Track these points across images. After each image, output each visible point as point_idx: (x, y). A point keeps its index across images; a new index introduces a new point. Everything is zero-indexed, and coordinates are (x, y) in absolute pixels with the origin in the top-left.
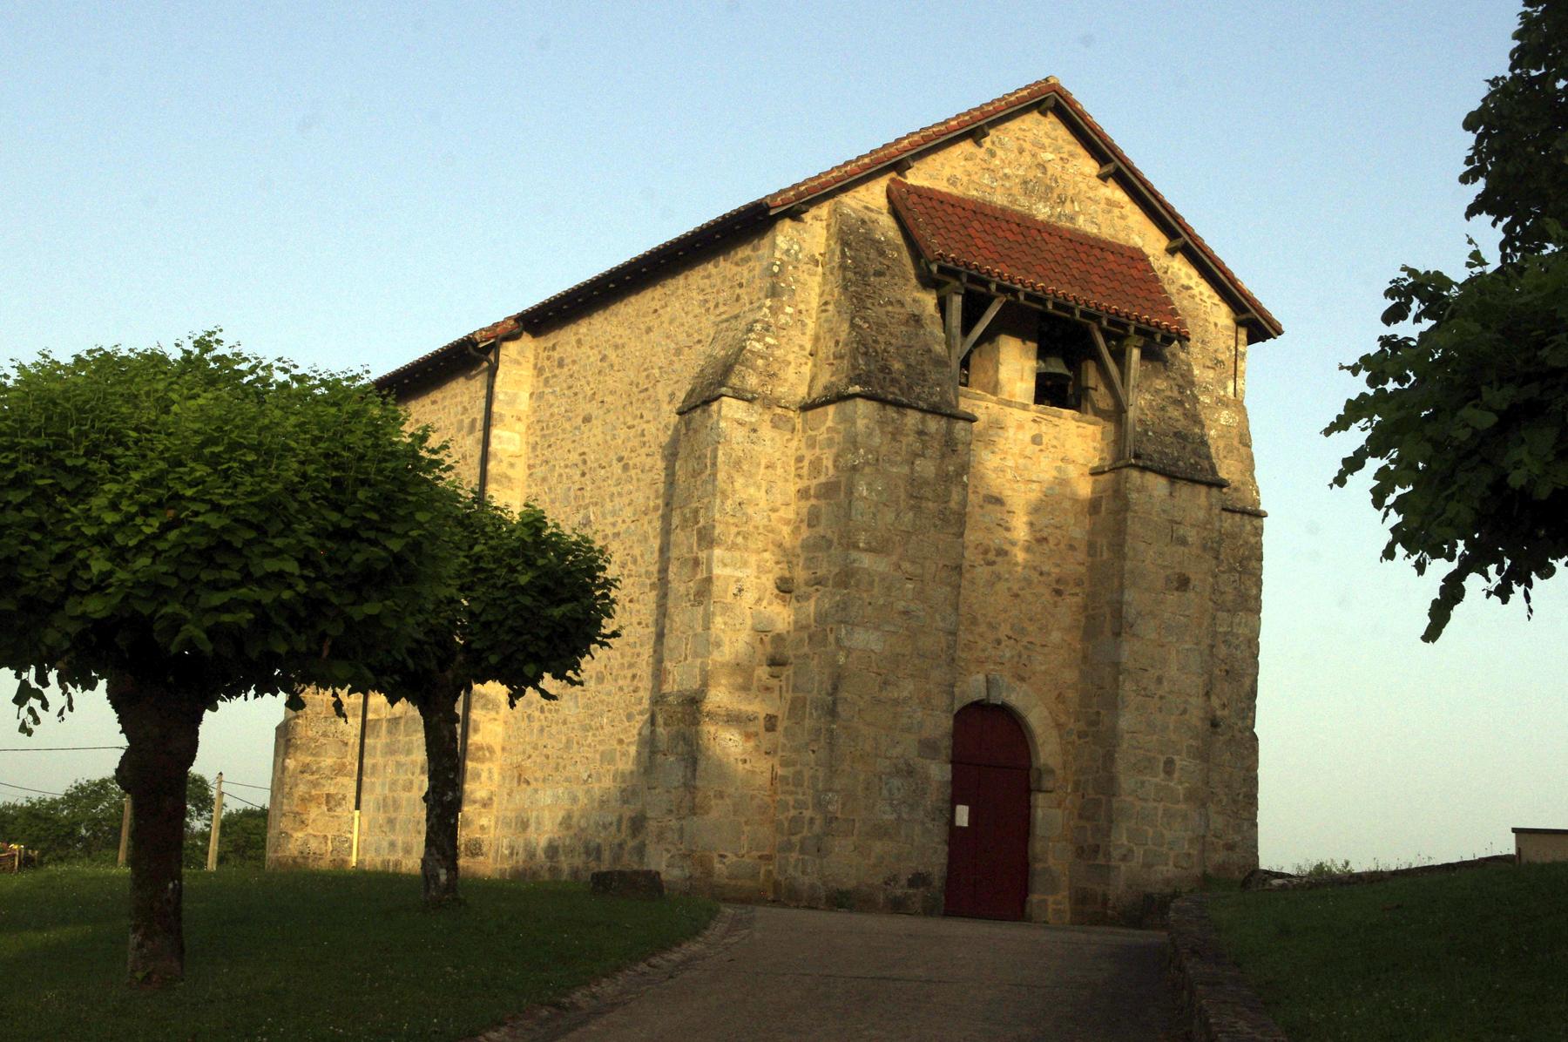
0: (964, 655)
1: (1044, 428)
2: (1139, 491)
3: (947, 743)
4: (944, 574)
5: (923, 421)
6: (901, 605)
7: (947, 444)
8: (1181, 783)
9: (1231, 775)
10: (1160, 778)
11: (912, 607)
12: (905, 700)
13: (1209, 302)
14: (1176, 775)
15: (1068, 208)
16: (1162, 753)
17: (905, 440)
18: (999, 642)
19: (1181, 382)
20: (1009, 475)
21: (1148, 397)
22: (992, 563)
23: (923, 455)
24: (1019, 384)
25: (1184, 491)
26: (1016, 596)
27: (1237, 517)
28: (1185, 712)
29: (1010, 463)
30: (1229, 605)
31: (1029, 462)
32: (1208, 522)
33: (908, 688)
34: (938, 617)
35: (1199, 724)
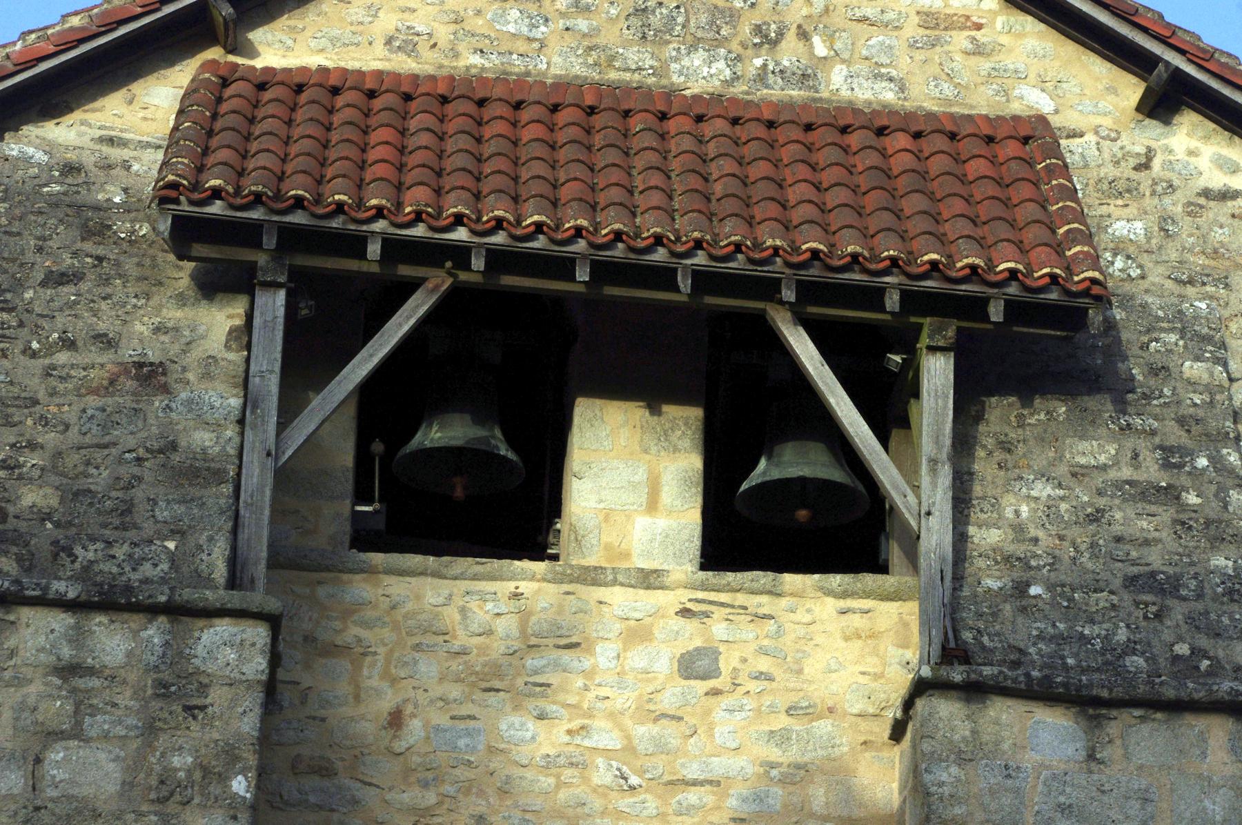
1: (719, 629)
2: (962, 759)
5: (78, 637)
7: (163, 690)
15: (789, 54)
19: (1175, 435)
20: (603, 775)
21: (1043, 490)
23: (76, 733)
25: (1141, 743)
31: (669, 730)
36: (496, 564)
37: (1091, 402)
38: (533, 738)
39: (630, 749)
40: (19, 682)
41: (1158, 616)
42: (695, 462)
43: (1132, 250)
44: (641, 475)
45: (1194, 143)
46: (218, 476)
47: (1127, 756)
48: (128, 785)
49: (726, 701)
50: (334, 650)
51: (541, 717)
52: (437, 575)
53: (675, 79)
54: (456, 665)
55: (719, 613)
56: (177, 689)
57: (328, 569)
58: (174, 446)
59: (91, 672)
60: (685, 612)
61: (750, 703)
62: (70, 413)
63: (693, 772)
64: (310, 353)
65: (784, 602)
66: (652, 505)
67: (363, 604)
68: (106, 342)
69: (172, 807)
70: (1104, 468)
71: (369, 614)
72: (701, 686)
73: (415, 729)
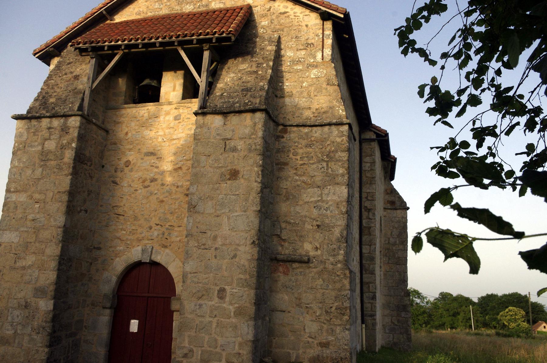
0: (129, 237)
3: (52, 288)
4: (57, 196)
5: (50, 123)
6: (30, 217)
8: (231, 304)
9: (323, 294)
10: (215, 301)
11: (38, 216)
12: (30, 267)
13: (301, 16)
14: (227, 299)
16: (216, 285)
17: (40, 134)
18: (151, 228)
19: (261, 61)
20: (160, 139)
21: (232, 75)
22: (149, 186)
23: (49, 139)
24: (172, 93)
25: (234, 119)
26: (162, 201)
27: (326, 129)
28: (235, 256)
29: (161, 133)
30: (319, 183)
31: (172, 130)
32: (252, 134)
33: (30, 260)
34: (52, 220)
35: (246, 264)
36: (144, 104)
37: (246, 57)
38: (149, 134)
39: (165, 135)
40: (42, 131)
41: (245, 96)
42: (182, 81)
43: (265, 27)
44: (172, 85)
45: (279, 4)
46: (81, 93)
47: (231, 123)
48: (56, 147)
49: (182, 124)
50: (119, 123)
51: (151, 130)
52: (136, 107)
53: (184, 10)
54: (138, 123)
55: (181, 108)
56: (65, 130)
57: (118, 109)
58: (76, 88)
59: (52, 128)
60: (176, 108)
61: (185, 124)
62: (63, 86)
63: (175, 137)
64: (99, 68)
65: (193, 104)
66: (174, 90)
67: (123, 115)
68: (71, 73)
69: (63, 150)
70: (245, 69)
71: (125, 116)
72: (177, 121)
73: (130, 134)
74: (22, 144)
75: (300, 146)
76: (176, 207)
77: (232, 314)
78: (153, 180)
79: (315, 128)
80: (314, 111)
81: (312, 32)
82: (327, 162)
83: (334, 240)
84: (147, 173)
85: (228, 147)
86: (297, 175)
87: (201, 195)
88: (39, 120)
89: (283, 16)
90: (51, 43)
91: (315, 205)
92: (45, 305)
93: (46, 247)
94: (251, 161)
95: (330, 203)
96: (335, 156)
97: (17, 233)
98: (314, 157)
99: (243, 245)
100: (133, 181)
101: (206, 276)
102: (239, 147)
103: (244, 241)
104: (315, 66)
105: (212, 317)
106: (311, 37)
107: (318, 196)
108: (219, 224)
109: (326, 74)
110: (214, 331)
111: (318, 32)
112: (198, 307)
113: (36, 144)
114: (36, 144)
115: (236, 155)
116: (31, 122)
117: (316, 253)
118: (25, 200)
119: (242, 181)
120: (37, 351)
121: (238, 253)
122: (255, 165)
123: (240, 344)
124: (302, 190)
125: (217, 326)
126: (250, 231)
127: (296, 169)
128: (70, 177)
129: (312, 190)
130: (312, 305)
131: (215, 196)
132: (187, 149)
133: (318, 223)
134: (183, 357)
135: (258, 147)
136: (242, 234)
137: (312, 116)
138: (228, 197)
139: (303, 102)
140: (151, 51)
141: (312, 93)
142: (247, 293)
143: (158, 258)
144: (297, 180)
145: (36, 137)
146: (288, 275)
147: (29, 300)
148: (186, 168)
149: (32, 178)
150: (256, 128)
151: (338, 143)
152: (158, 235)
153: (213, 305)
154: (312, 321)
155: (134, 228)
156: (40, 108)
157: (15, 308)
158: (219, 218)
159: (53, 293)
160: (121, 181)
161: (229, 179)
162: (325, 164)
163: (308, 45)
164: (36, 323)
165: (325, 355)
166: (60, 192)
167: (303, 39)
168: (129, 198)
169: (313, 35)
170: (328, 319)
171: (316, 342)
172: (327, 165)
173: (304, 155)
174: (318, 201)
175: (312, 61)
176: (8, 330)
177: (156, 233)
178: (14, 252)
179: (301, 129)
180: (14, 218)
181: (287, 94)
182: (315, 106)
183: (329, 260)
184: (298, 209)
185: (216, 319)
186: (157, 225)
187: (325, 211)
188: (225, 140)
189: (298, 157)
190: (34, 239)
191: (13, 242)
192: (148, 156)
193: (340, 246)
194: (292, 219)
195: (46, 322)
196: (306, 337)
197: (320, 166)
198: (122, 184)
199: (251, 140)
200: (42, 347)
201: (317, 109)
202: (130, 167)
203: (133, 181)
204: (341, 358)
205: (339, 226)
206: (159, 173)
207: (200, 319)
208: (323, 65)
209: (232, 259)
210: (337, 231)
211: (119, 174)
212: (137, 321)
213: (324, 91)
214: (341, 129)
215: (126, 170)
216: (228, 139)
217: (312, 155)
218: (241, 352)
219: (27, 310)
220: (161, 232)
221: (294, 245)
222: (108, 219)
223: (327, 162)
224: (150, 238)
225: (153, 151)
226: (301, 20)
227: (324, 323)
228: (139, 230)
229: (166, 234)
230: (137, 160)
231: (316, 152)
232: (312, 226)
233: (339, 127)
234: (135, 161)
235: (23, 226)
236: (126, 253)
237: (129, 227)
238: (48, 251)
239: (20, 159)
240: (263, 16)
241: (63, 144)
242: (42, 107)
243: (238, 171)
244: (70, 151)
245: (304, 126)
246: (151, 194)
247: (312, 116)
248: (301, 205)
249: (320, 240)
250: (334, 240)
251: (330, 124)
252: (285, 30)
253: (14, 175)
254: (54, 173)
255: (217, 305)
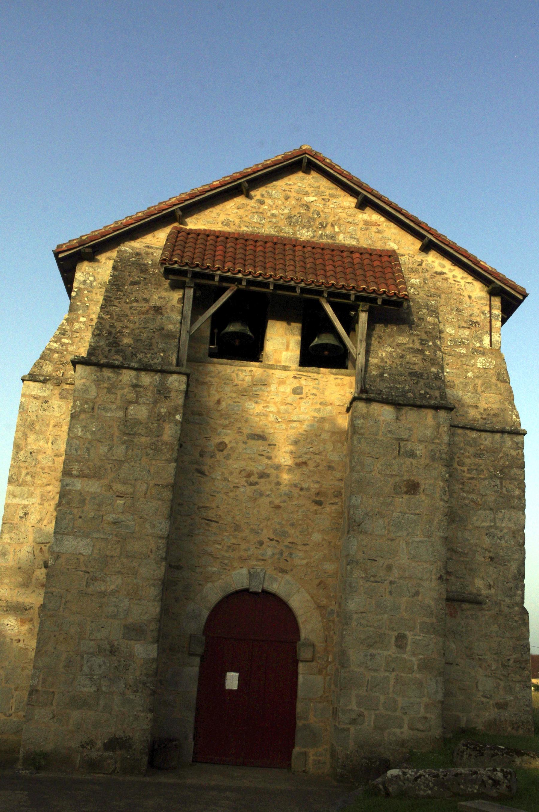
0: (227, 555)
1: (303, 382)
2: (364, 418)
3: (153, 626)
4: (154, 491)
5: (137, 378)
6: (110, 517)
7: (159, 392)
8: (414, 654)
9: (499, 644)
10: (392, 651)
11: (122, 517)
12: (113, 593)
13: (462, 282)
14: (409, 648)
15: (329, 231)
16: (393, 629)
17: (120, 393)
18: (261, 543)
19: (424, 336)
20: (272, 418)
21: (389, 349)
22: (256, 483)
23: (137, 402)
24: (284, 353)
25: (411, 416)
26: (278, 507)
27: (498, 436)
28: (417, 593)
29: (272, 409)
30: (492, 505)
31: (290, 408)
32: (436, 438)
33: (114, 582)
34: (147, 525)
35: (432, 603)
36: (246, 363)
37: (402, 327)
38: (255, 408)
39: (279, 412)
40: (123, 389)
41: (417, 383)
42: (299, 338)
43: (416, 287)
44: (284, 341)
45: (433, 259)
46: (174, 337)
47: (406, 419)
48: (149, 416)
49: (304, 401)
50: (203, 383)
51: (256, 403)
52: (231, 365)
53: (298, 236)
54: (235, 389)
55: (303, 378)
56: (163, 392)
57: (202, 362)
58: (163, 329)
59: (141, 387)
60: (295, 377)
61: (310, 401)
62: (136, 319)
63: (295, 418)
64: (200, 305)
65: (320, 376)
66: (287, 349)
67: (210, 372)
68: (146, 300)
69: (161, 422)
70: (405, 344)
71: (213, 374)
72: (298, 396)
73: (223, 404)
74: (87, 403)
75: (467, 454)
76: (301, 517)
77: (415, 668)
78: (263, 475)
79: (484, 435)
80: (482, 411)
81: (477, 307)
82: (501, 479)
83: (510, 576)
84: (253, 464)
85: (402, 450)
86: (464, 492)
87: (369, 509)
88: (116, 370)
89: (439, 278)
90: (88, 240)
91: (487, 532)
92: (144, 651)
93: (139, 565)
94: (435, 473)
95: (505, 531)
96: (509, 472)
97: (88, 540)
98: (485, 471)
99: (427, 579)
100: (231, 473)
101: (379, 617)
102: (418, 452)
103: (429, 574)
104: (482, 352)
105: (388, 671)
106: (475, 314)
107: (491, 521)
108: (394, 551)
109: (495, 366)
110: (391, 690)
111: (484, 308)
112: (369, 658)
113: (114, 407)
114: (114, 407)
115: (414, 461)
116: (101, 371)
117: (489, 591)
118: (99, 490)
119: (423, 497)
120: (136, 718)
121: (421, 590)
122: (440, 478)
123: (427, 706)
124: (471, 512)
125: (396, 683)
126: (435, 562)
127: (463, 484)
128: (174, 465)
129: (484, 512)
130: (486, 657)
131: (388, 512)
132: (314, 438)
133: (491, 555)
134: (350, 724)
135: (444, 456)
136: (425, 566)
137: (479, 417)
138: (406, 516)
139: (467, 398)
140: (279, 295)
141: (479, 388)
142: (434, 641)
143: (274, 588)
144: (464, 498)
145: (113, 396)
146: (455, 617)
147: (116, 643)
148: (314, 465)
149: (108, 459)
150: (440, 432)
151: (513, 457)
152: (274, 554)
153: (390, 656)
154: (486, 676)
155: (234, 541)
156: (110, 351)
157: (92, 653)
158: (393, 542)
159: (155, 634)
160: (211, 470)
161: (406, 493)
162: (498, 482)
163: (472, 324)
164: (132, 677)
165: (502, 718)
166: (158, 485)
167: (466, 314)
168: (225, 497)
169: (478, 311)
170: (505, 673)
171: (491, 702)
172: (501, 483)
173: (472, 467)
174: (491, 526)
175: (478, 345)
176: (84, 686)
177: (270, 552)
178: (84, 569)
179: (468, 432)
180: (80, 517)
181: (448, 384)
182: (483, 405)
183: (504, 601)
184: (467, 535)
185: (394, 674)
186: (272, 540)
187: (499, 541)
188: (399, 440)
189: (465, 469)
190: (118, 551)
191: (81, 554)
192: (254, 439)
193: (517, 584)
194: (460, 547)
195: (147, 675)
196: (478, 696)
197: (493, 484)
198: (213, 476)
199: (434, 446)
200: (143, 711)
201: (485, 410)
202: (225, 452)
203: (231, 473)
204: (523, 723)
205: (516, 560)
206: (271, 467)
207: (372, 674)
208: (492, 353)
209: (413, 596)
210: (514, 566)
211: (208, 461)
212: (236, 675)
213: (493, 387)
214: (515, 439)
215: (219, 456)
216: (403, 440)
217: (482, 467)
218: (428, 715)
219: (114, 658)
220: (277, 551)
221: (462, 580)
222: (192, 525)
223: (501, 479)
224: (260, 557)
225: (261, 434)
226: (462, 287)
227: (501, 680)
228: (243, 546)
229: (286, 554)
230: (237, 443)
231: (486, 465)
232: (484, 557)
233: (512, 436)
234: (233, 444)
235: (98, 531)
236: (223, 577)
237: (226, 540)
238: (144, 571)
239: (85, 427)
240: (414, 271)
241: (160, 412)
242: (113, 349)
243: (418, 484)
244: (172, 425)
245: (472, 429)
246: (261, 494)
247: (479, 417)
248: (470, 531)
249: (494, 576)
250: (510, 576)
251: (503, 432)
252: (443, 296)
253: (76, 450)
254: (148, 455)
255: (394, 656)
